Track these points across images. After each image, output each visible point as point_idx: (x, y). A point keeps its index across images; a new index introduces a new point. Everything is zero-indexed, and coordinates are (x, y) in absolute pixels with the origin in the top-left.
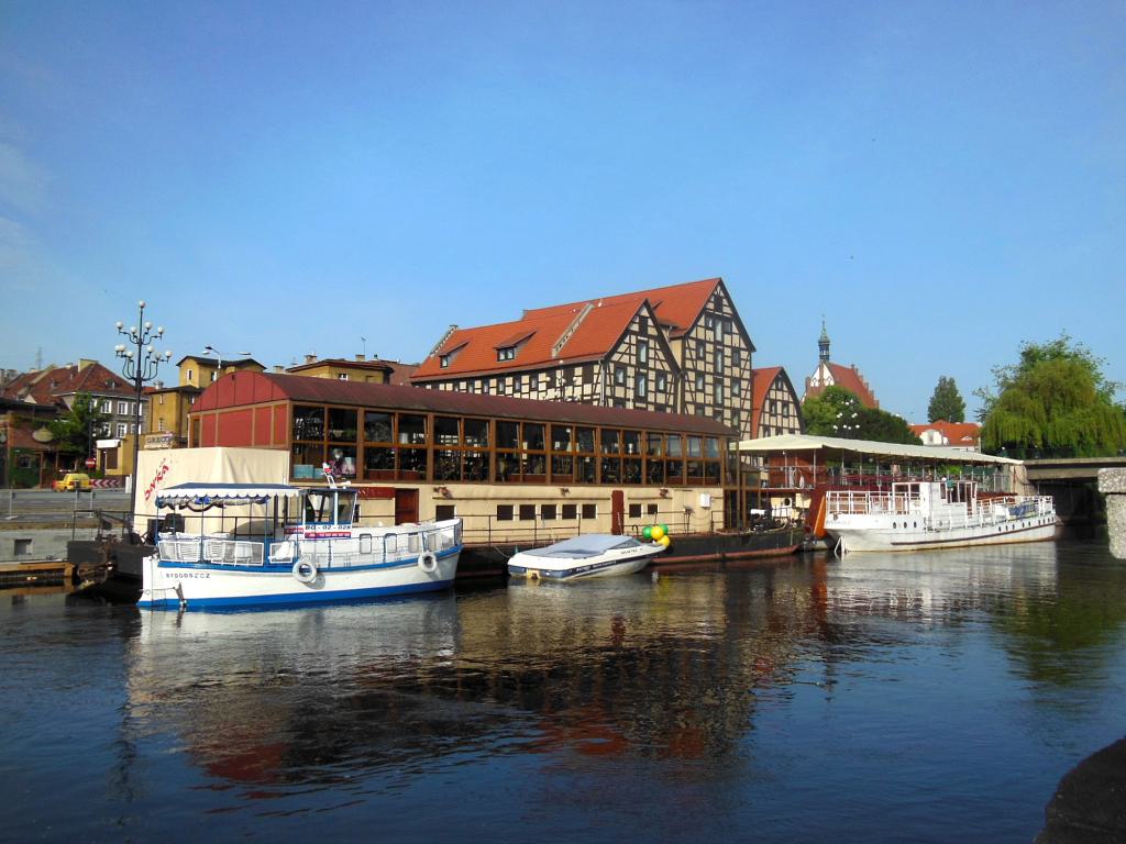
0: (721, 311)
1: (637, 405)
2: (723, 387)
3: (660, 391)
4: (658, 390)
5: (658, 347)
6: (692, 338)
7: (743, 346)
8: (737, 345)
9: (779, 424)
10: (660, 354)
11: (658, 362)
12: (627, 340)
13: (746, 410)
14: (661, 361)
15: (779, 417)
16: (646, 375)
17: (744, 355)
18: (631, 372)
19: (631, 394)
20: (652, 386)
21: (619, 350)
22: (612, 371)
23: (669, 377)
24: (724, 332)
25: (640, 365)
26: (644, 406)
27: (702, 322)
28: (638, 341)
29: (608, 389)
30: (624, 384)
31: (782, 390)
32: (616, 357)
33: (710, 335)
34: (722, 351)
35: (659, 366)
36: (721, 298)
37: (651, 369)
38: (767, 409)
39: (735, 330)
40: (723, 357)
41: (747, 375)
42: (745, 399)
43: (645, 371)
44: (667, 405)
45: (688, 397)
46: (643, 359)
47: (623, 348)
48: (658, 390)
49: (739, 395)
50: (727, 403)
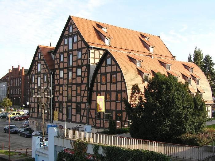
5: (44, 63)
8: (80, 47)
11: (44, 70)
12: (35, 65)
13: (85, 84)
14: (45, 69)
15: (108, 84)
17: (84, 51)
27: (62, 44)
33: (66, 48)
35: (44, 72)
38: (99, 81)
39: (79, 39)
40: (73, 56)
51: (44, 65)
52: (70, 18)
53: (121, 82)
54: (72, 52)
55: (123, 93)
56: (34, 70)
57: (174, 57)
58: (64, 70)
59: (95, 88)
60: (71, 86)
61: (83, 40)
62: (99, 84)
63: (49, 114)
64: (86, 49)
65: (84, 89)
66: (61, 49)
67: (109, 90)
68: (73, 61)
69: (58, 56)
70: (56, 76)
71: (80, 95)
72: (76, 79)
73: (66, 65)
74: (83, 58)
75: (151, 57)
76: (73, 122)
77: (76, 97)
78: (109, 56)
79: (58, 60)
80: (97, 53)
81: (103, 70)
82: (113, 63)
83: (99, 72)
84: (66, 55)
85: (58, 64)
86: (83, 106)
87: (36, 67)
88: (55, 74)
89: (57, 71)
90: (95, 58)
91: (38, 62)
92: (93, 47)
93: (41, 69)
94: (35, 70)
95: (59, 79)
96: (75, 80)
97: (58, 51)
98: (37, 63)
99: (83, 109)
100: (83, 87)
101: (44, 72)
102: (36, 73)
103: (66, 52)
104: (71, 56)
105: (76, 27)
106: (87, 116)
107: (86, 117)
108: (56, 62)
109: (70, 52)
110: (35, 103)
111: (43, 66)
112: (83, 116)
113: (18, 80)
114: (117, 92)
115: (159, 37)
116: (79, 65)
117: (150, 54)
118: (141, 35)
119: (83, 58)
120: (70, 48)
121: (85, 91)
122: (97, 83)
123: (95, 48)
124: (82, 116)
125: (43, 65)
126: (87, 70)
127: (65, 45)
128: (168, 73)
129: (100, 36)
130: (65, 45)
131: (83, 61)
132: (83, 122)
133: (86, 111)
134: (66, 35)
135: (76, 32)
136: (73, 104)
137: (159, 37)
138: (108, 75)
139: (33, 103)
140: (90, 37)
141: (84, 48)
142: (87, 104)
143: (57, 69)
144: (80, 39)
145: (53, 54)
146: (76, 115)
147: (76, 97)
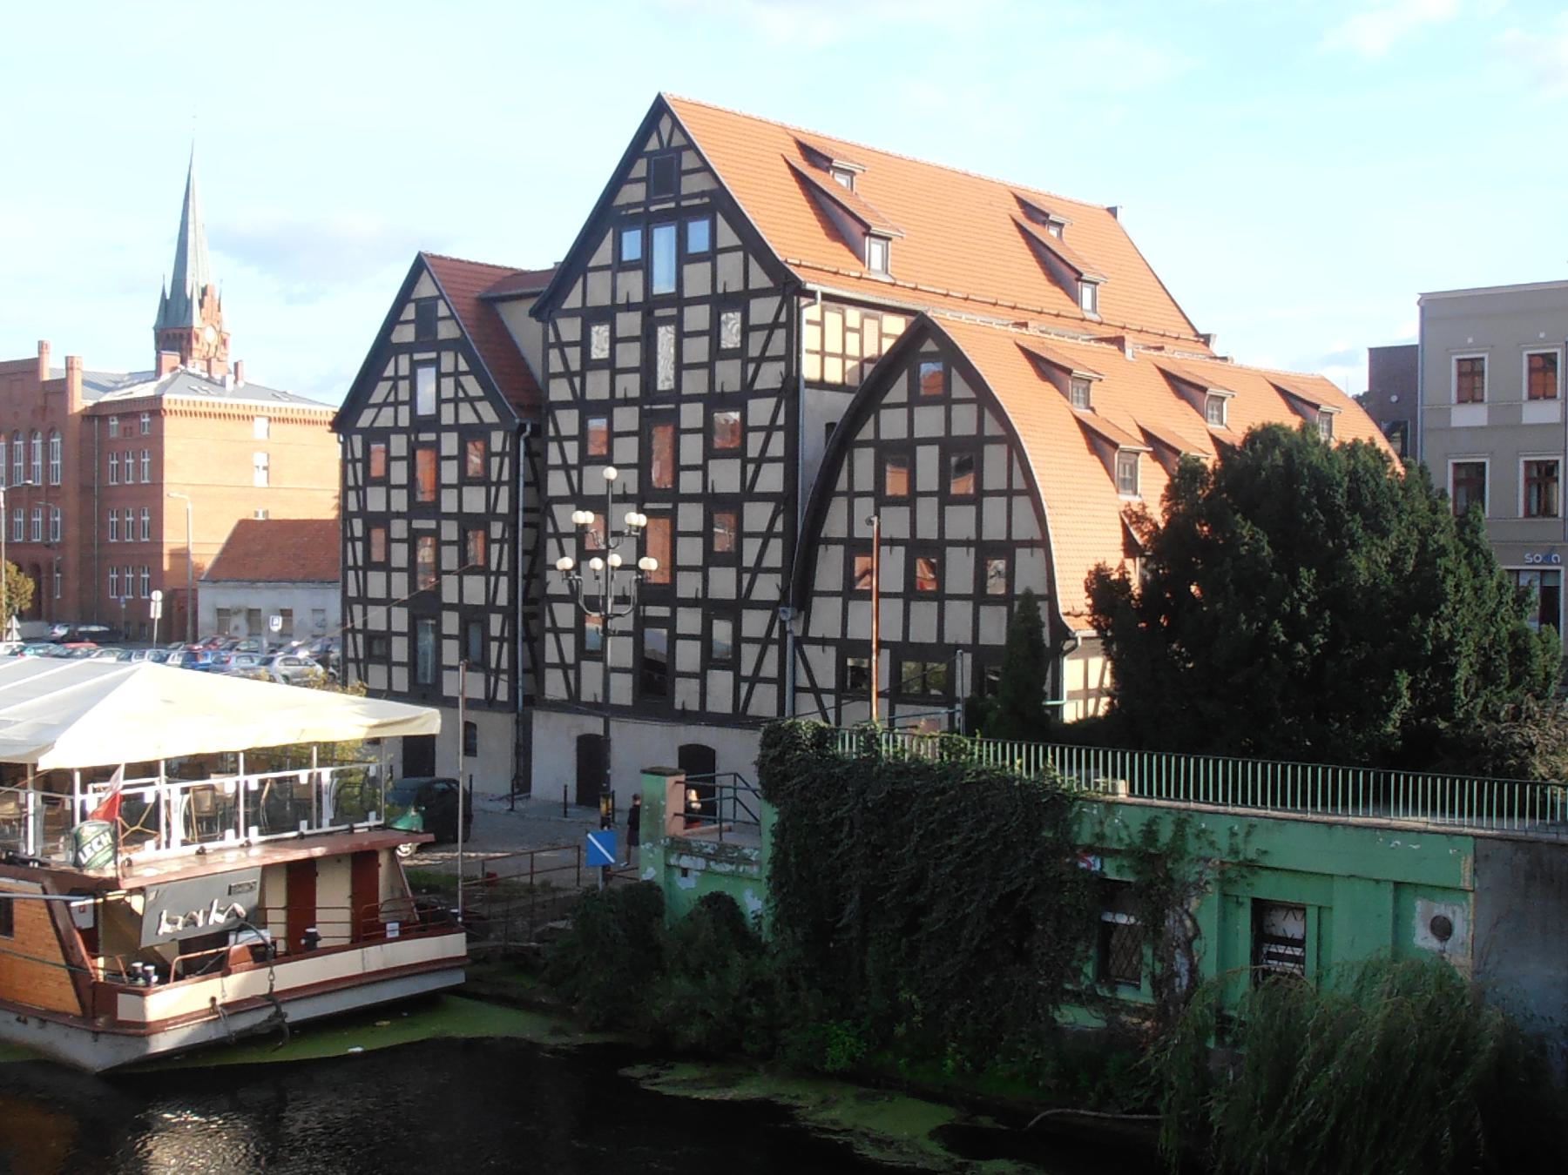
0: (678, 198)
1: (417, 524)
2: (678, 432)
3: (473, 482)
4: (464, 480)
5: (463, 366)
6: (571, 313)
7: (759, 279)
8: (735, 286)
9: (927, 530)
10: (472, 387)
11: (465, 409)
12: (390, 371)
13: (765, 497)
14: (471, 401)
15: (927, 509)
16: (436, 446)
17: (762, 310)
18: (399, 444)
19: (400, 502)
20: (450, 473)
21: (372, 401)
22: (358, 454)
23: (497, 441)
24: (684, 257)
25: (420, 423)
26: (432, 524)
27: (603, 255)
28: (414, 365)
29: (352, 495)
30: (385, 481)
31: (945, 400)
32: (365, 420)
34: (678, 321)
35: (467, 416)
36: (680, 150)
37: (449, 428)
38: (865, 481)
39: (727, 236)
40: (680, 336)
41: (770, 376)
42: (762, 459)
43: (431, 437)
44: (491, 514)
45: (557, 484)
46: (426, 406)
47: (381, 392)
48: (464, 480)
49: (740, 453)
50: (690, 483)
51: (463, 379)
52: (660, 108)
53: (1009, 493)
54: (672, 311)
55: (1022, 555)
56: (385, 404)
57: (1206, 340)
58: (617, 412)
59: (835, 525)
60: (669, 506)
61: (753, 245)
62: (864, 506)
63: (498, 671)
64: (776, 300)
65: (763, 528)
66: (598, 290)
67: (934, 536)
68: (680, 366)
69: (570, 329)
70: (553, 449)
71: (733, 559)
72: (704, 468)
73: (630, 385)
74: (754, 351)
75: (1122, 347)
76: (686, 717)
77: (704, 570)
78: (929, 346)
79: (574, 355)
80: (833, 320)
81: (892, 425)
82: (960, 389)
83: (867, 432)
84: (629, 323)
85: (568, 374)
86: (755, 623)
87: (404, 386)
88: (552, 432)
89: (568, 421)
90: (823, 354)
91: (417, 357)
92: (819, 289)
93: (440, 401)
94: (391, 404)
95: (579, 468)
96: (700, 473)
97: (573, 300)
98: (404, 361)
99: (495, 639)
100: (757, 516)
101: (463, 421)
102: (404, 421)
103: (629, 307)
104: (665, 336)
105: (706, 168)
106: (780, 681)
107: (773, 690)
108: (556, 365)
109: (659, 313)
110: (388, 602)
111: (458, 385)
112: (755, 679)
113: (38, 442)
114: (984, 550)
115: (1113, 211)
116: (727, 389)
117: (1119, 333)
118: (1022, 203)
119: (754, 351)
120: (663, 284)
121: (767, 536)
122: (852, 495)
123: (826, 297)
124: (746, 679)
125: (456, 374)
126: (781, 421)
127: (619, 265)
128: (1216, 441)
129: (839, 222)
130: (619, 265)
131: (751, 368)
132: (752, 711)
133: (773, 651)
134: (630, 206)
135: (701, 194)
136: (681, 611)
137: (1113, 211)
138: (928, 459)
139: (377, 602)
140: (791, 233)
141: (762, 293)
142: (787, 614)
143: (565, 405)
144: (736, 241)
145: (535, 313)
146: (702, 676)
147: (704, 570)
